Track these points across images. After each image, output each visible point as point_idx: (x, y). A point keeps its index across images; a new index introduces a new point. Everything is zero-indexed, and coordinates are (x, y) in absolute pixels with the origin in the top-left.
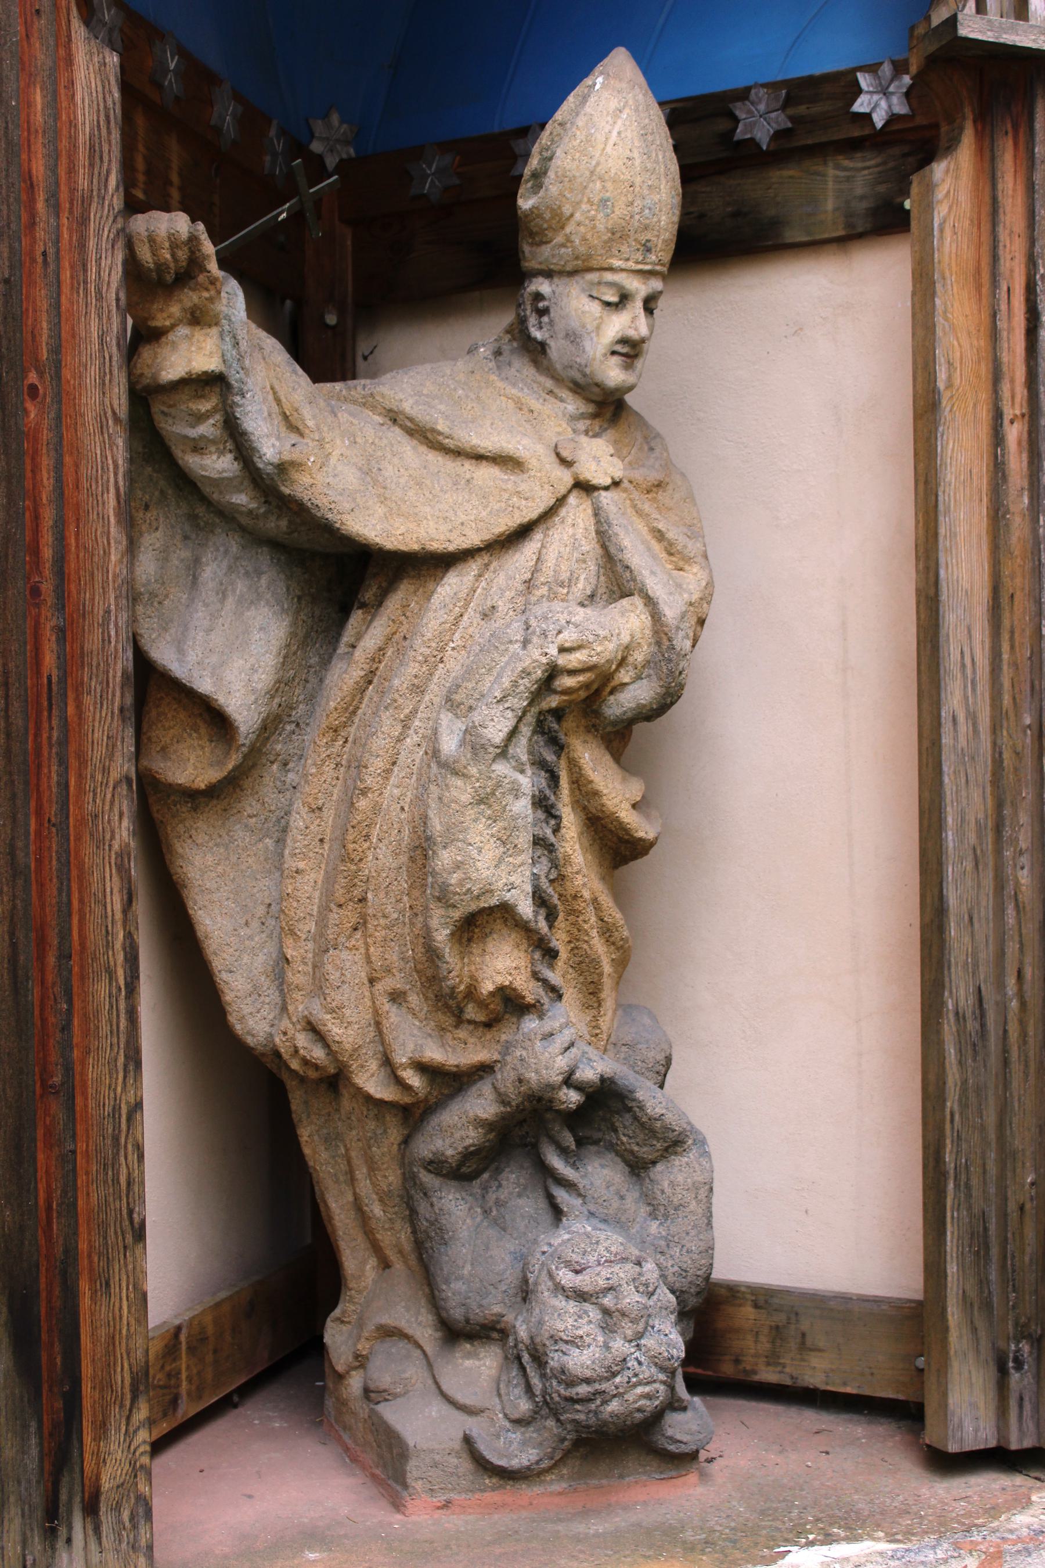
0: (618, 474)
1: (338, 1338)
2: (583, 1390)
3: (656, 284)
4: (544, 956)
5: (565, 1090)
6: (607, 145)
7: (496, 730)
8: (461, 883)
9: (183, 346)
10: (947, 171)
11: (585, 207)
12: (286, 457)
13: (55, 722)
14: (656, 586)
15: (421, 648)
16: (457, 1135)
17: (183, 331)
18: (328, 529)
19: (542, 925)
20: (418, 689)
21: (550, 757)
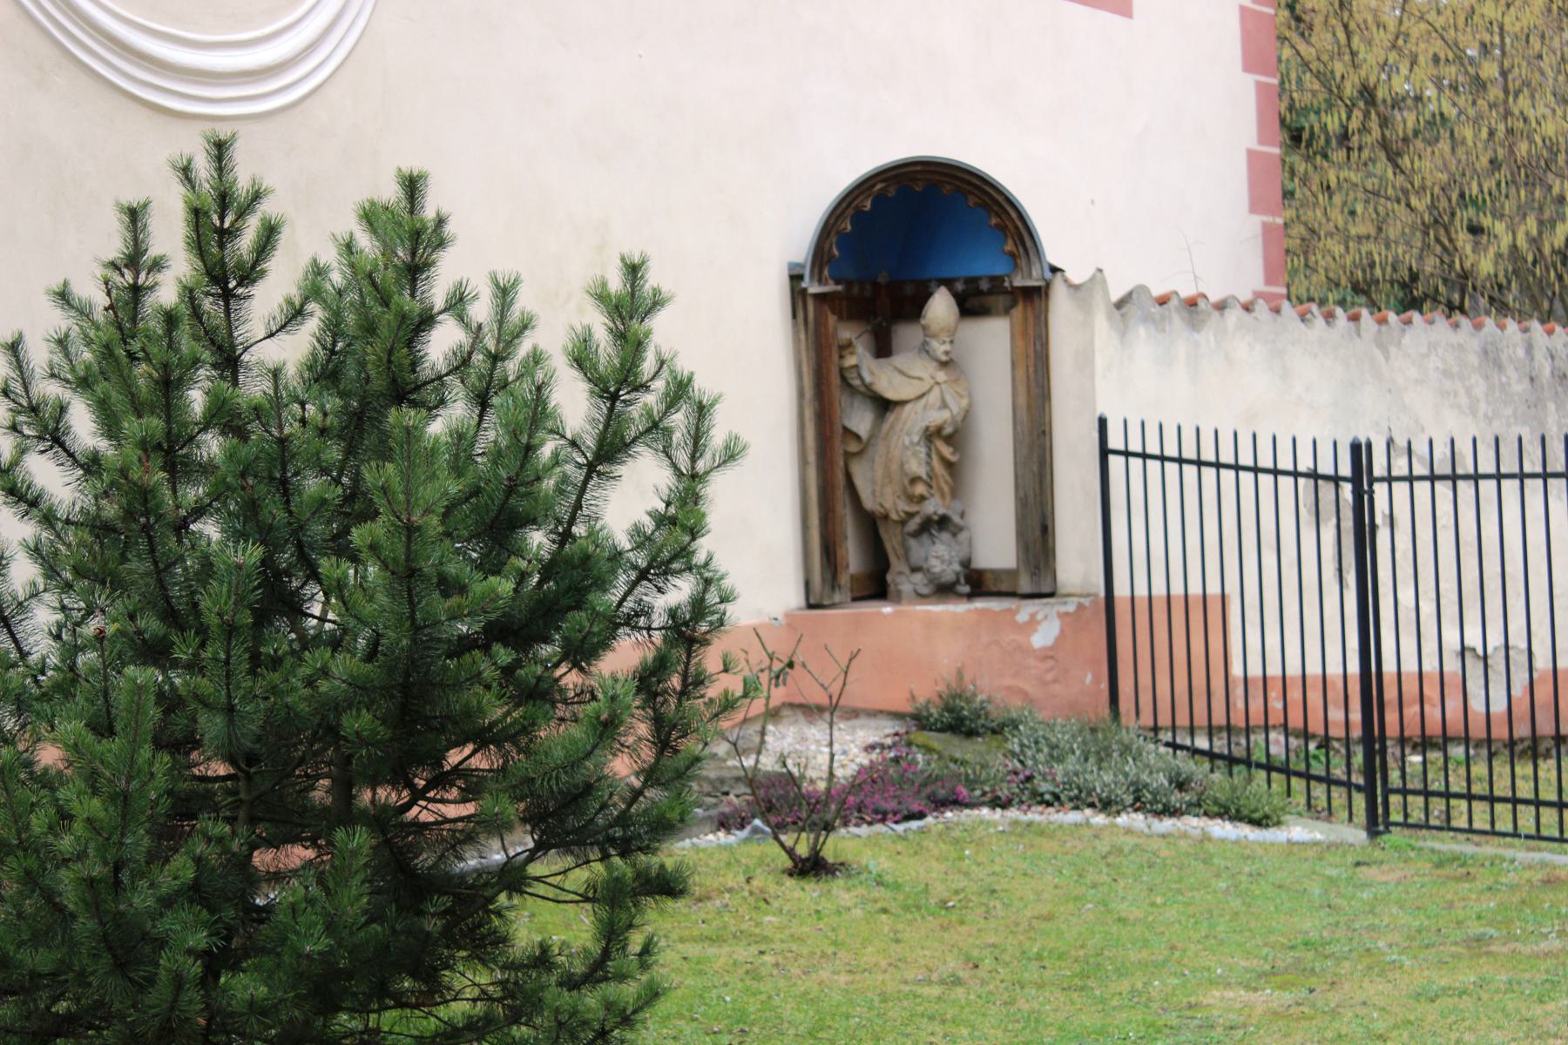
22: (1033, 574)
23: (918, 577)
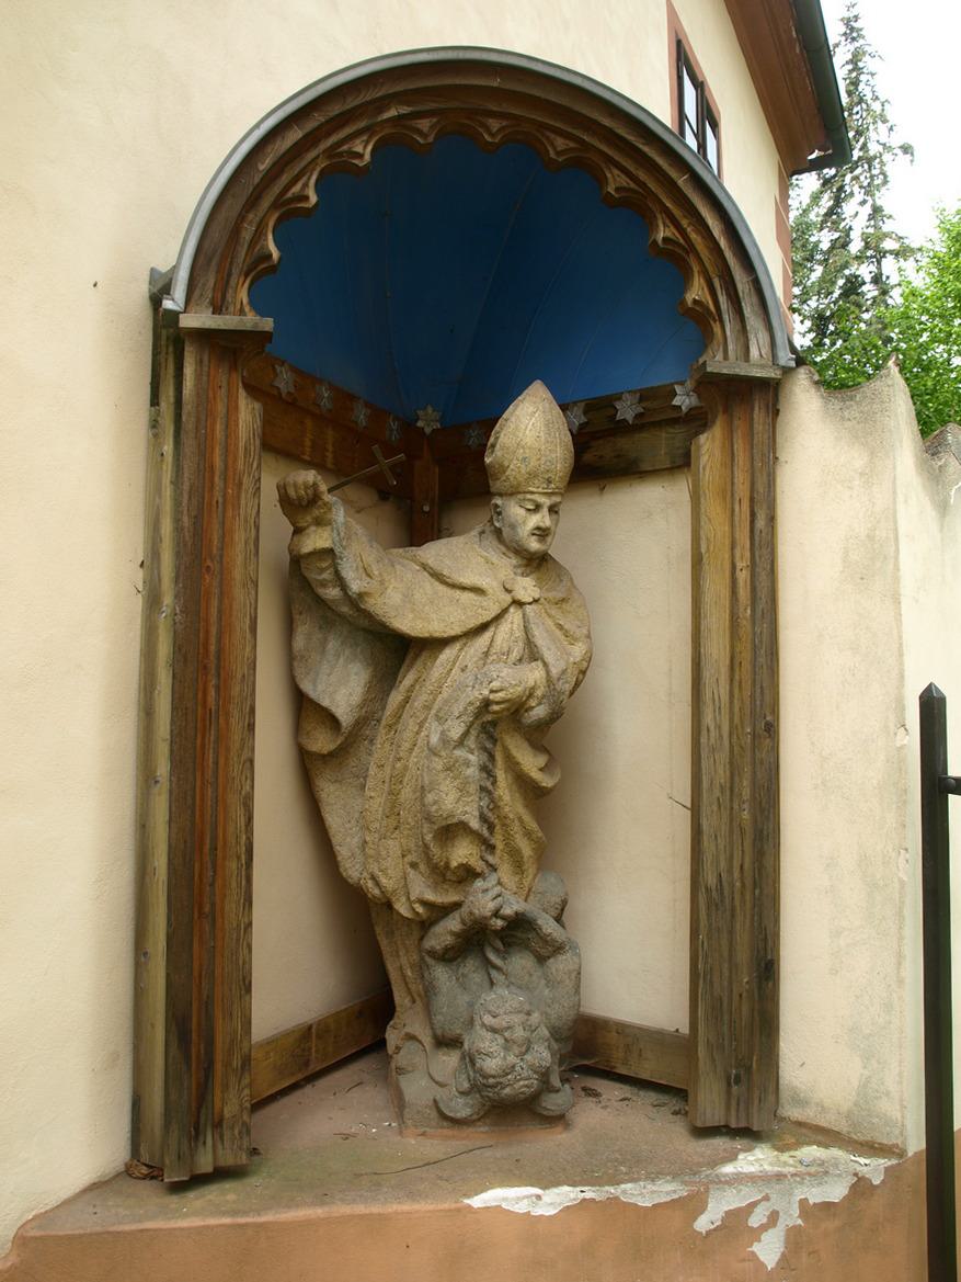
0: (537, 597)
1: (392, 1037)
2: (491, 1081)
3: (557, 499)
4: (487, 848)
5: (494, 919)
6: (531, 429)
7: (456, 731)
8: (437, 811)
9: (312, 536)
10: (707, 439)
11: (515, 462)
12: (363, 590)
13: (212, 732)
14: (549, 656)
15: (429, 687)
16: (442, 939)
17: (313, 528)
18: (383, 625)
19: (485, 833)
20: (428, 708)
21: (489, 745)
22: (730, 1082)
23: (449, 1060)
